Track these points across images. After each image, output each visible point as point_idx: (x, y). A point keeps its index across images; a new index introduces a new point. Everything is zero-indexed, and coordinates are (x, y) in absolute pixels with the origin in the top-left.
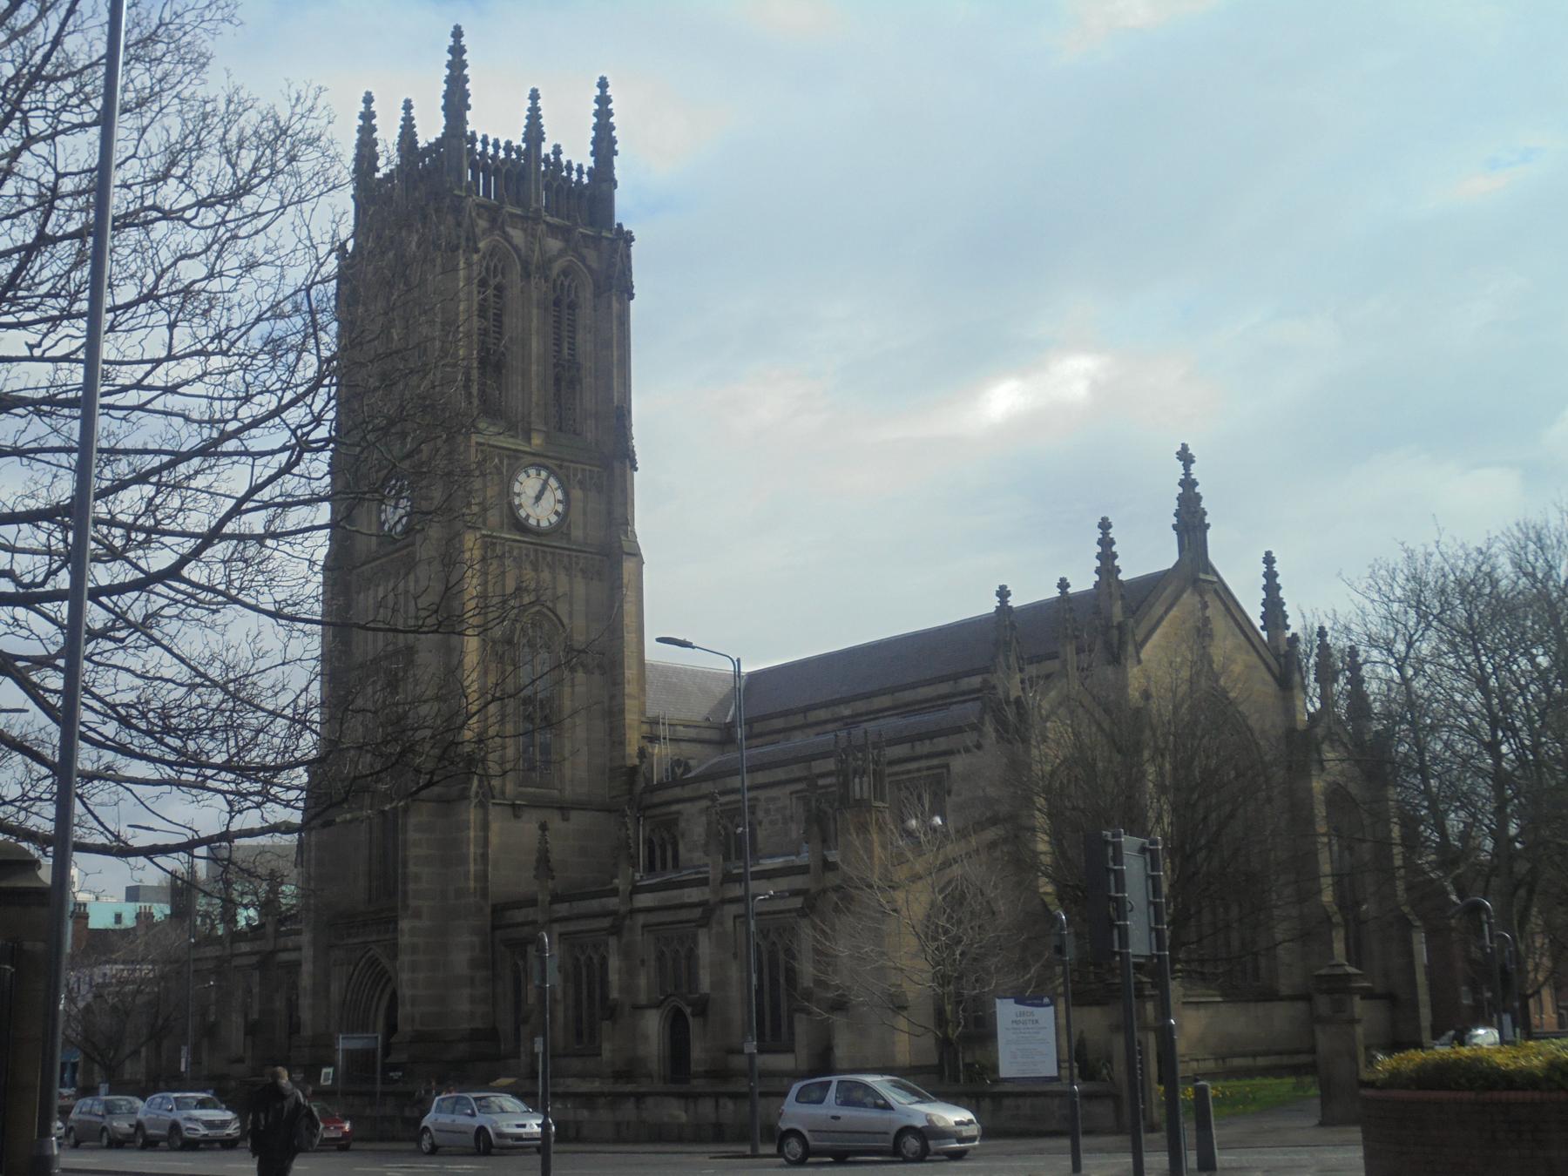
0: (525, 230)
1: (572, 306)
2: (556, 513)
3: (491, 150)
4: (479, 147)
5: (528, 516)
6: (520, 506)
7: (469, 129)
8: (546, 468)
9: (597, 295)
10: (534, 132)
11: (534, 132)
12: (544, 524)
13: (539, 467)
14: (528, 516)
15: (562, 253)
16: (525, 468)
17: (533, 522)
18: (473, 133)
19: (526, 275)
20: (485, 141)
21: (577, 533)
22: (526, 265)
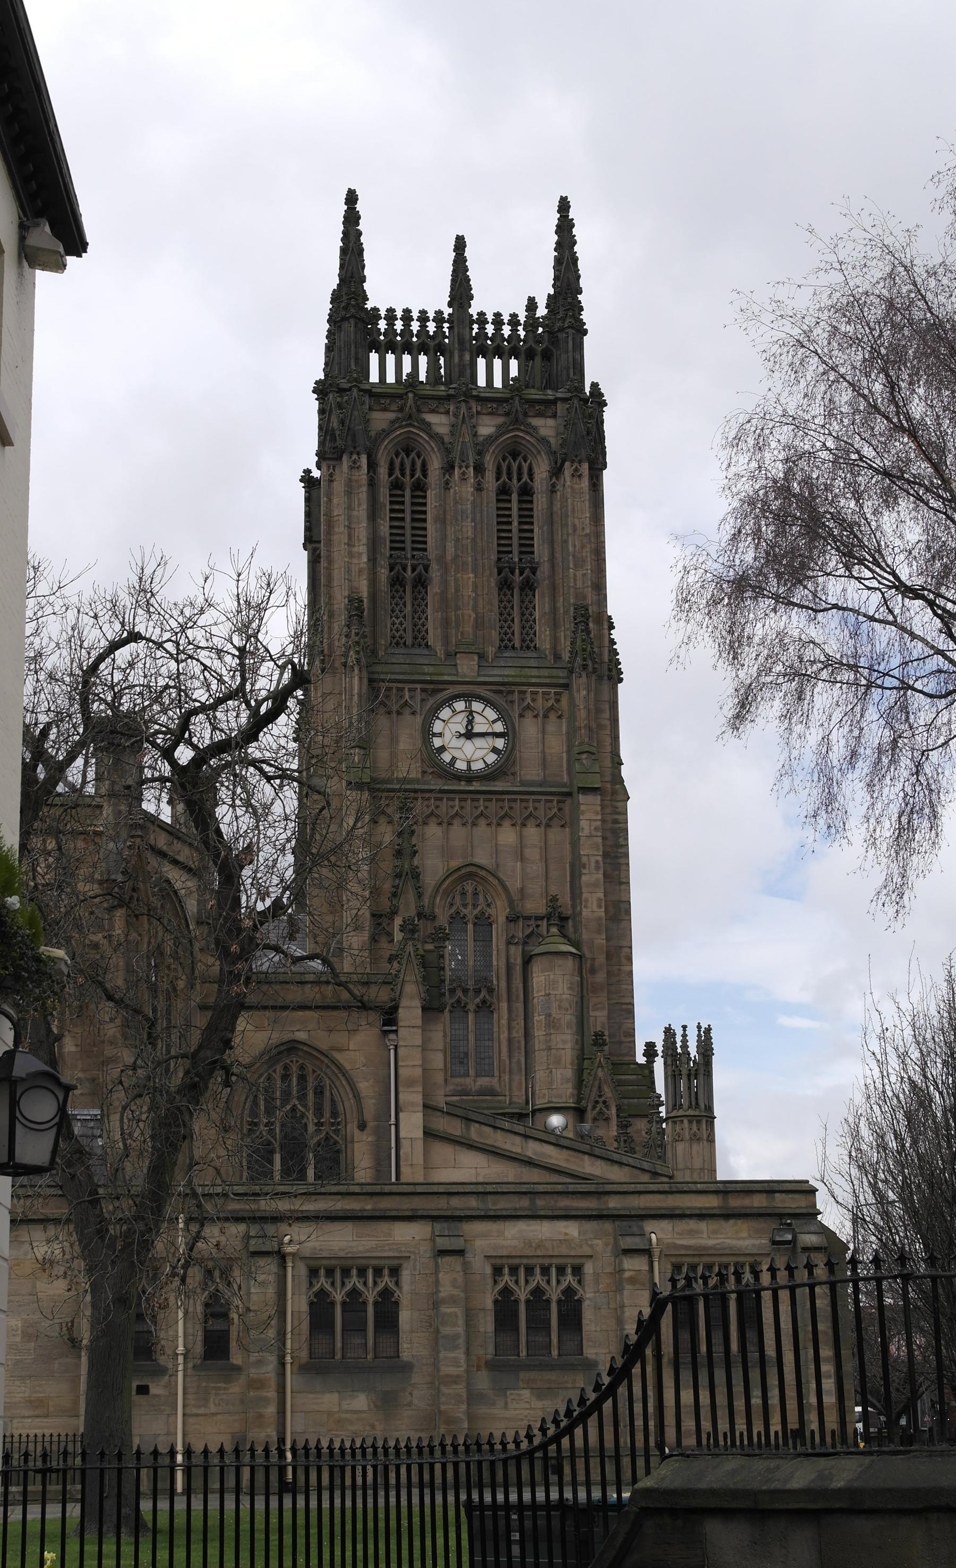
0: (447, 413)
1: (526, 492)
2: (495, 750)
3: (399, 326)
4: (382, 325)
5: (454, 759)
6: (442, 749)
7: (369, 305)
8: (480, 698)
9: (556, 472)
12: (477, 766)
13: (468, 697)
14: (454, 759)
15: (501, 430)
16: (448, 701)
17: (461, 765)
18: (376, 310)
19: (449, 468)
20: (391, 313)
21: (530, 771)
22: (447, 450)
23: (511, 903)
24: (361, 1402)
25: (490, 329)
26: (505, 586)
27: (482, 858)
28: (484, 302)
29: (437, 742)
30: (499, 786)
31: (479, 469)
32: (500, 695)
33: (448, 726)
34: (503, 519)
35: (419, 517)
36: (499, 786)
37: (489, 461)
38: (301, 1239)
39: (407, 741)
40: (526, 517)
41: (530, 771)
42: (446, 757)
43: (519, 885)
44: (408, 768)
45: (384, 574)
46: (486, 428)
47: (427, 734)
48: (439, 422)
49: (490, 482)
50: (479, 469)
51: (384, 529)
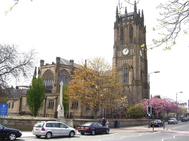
10: (126, 12)
11: (126, 12)
13: (126, 48)
23: (129, 66)
24: (51, 110)
25: (128, 14)
26: (130, 37)
27: (127, 63)
28: (128, 12)
29: (123, 53)
30: (128, 56)
31: (127, 27)
32: (129, 48)
33: (124, 51)
34: (130, 31)
35: (123, 33)
36: (128, 56)
37: (128, 26)
38: (48, 98)
39: (121, 53)
40: (132, 31)
41: (131, 54)
42: (124, 54)
43: (131, 65)
44: (121, 56)
45: (119, 38)
46: (128, 23)
47: (122, 52)
48: (124, 24)
49: (128, 28)
50: (127, 27)
51: (120, 34)
